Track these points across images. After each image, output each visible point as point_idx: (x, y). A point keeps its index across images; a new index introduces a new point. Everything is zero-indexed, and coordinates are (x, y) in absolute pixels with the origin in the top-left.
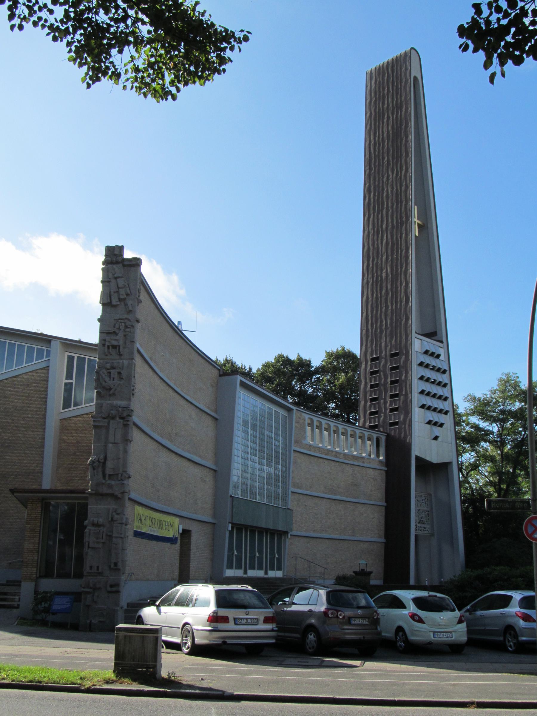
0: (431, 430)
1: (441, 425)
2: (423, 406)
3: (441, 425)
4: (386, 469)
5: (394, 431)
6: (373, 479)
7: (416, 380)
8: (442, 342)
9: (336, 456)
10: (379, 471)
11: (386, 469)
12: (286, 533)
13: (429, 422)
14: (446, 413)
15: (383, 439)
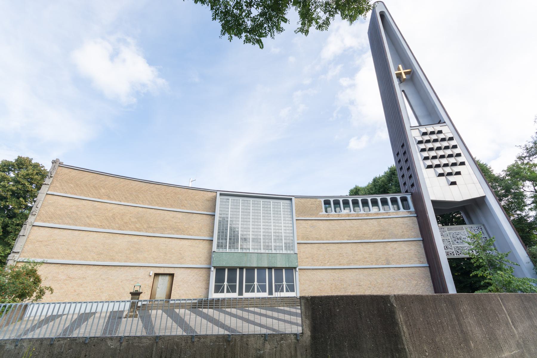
0: (447, 180)
1: (458, 173)
2: (430, 167)
3: (458, 173)
4: (416, 215)
5: (414, 190)
6: (403, 224)
7: (419, 154)
8: (445, 122)
9: (358, 216)
10: (408, 218)
11: (416, 215)
12: (295, 268)
13: (441, 175)
14: (463, 164)
15: (409, 197)
